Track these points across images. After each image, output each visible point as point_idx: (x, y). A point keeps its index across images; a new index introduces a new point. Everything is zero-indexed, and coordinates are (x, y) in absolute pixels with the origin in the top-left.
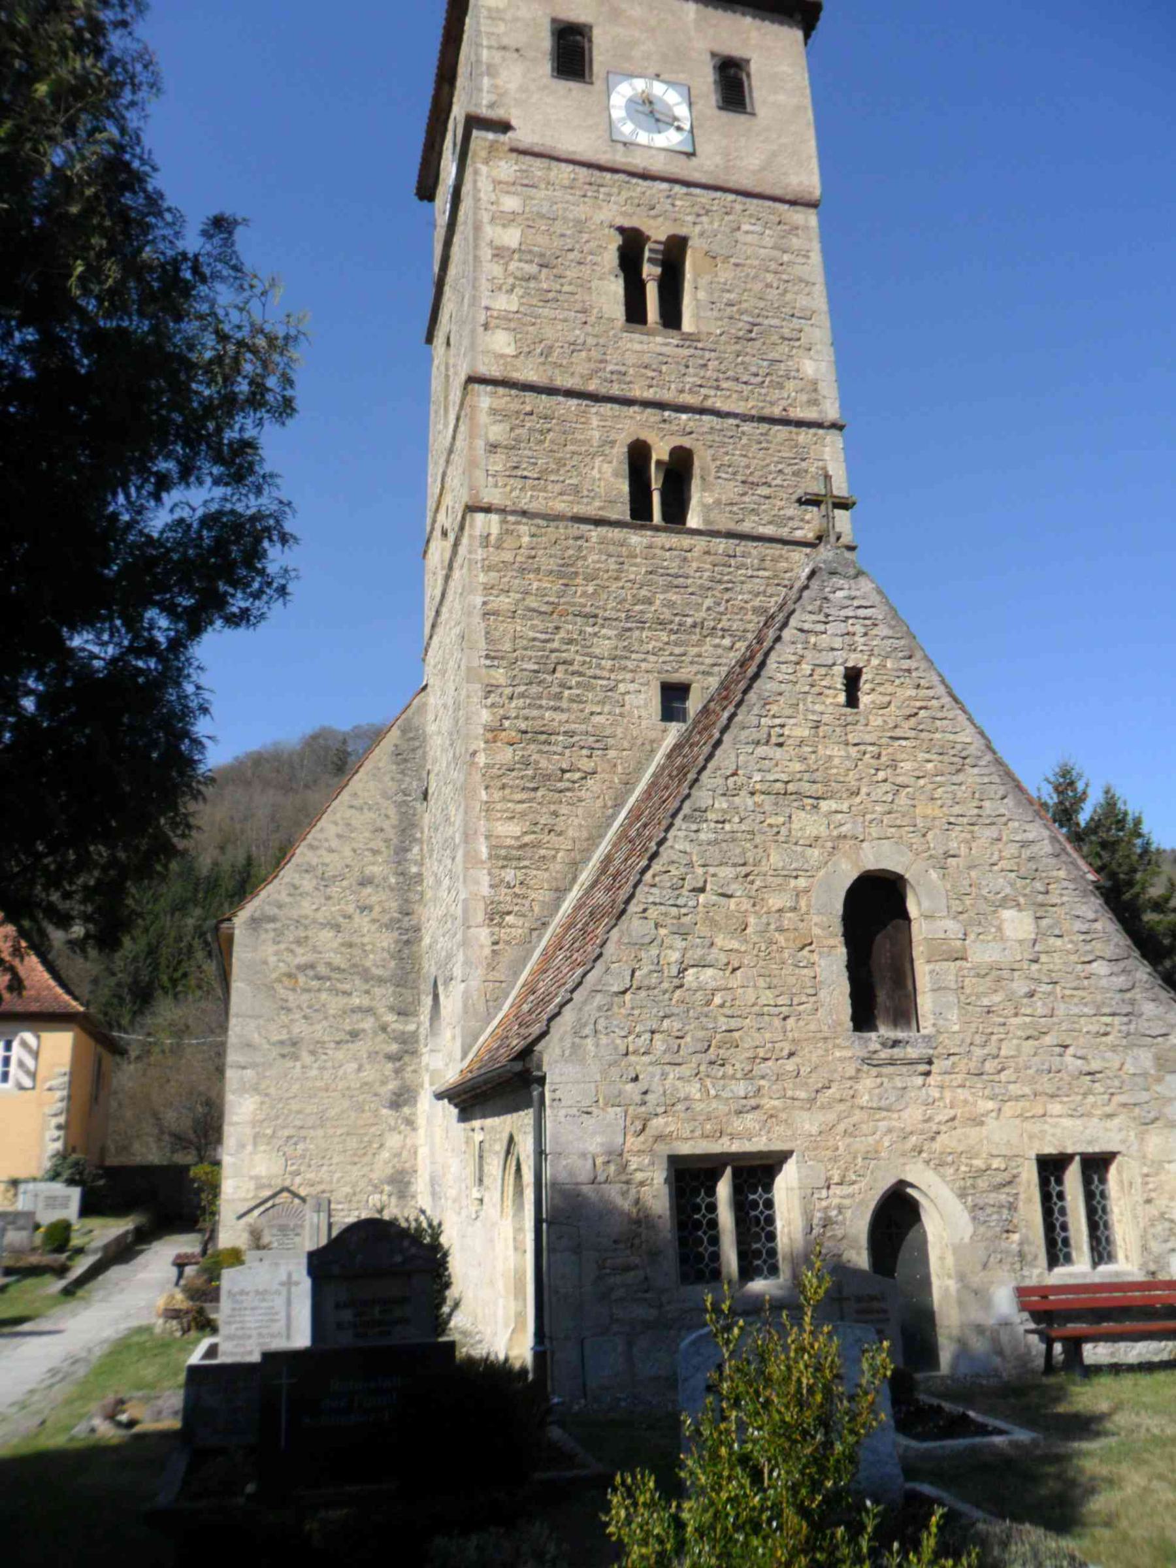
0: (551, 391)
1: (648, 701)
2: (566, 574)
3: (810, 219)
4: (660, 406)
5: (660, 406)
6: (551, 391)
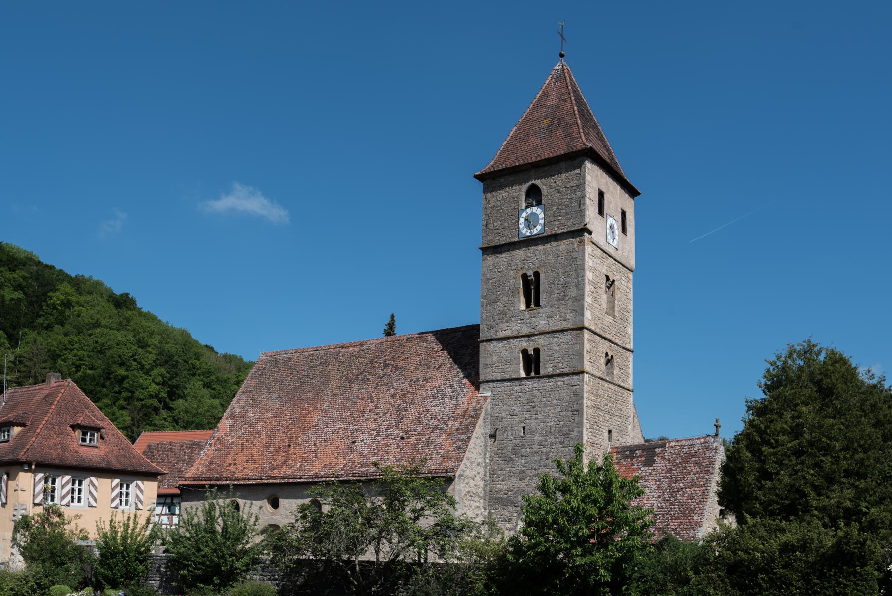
0: (595, 333)
1: (606, 435)
2: (596, 395)
3: (631, 276)
4: (610, 341)
5: (610, 341)
6: (595, 333)
